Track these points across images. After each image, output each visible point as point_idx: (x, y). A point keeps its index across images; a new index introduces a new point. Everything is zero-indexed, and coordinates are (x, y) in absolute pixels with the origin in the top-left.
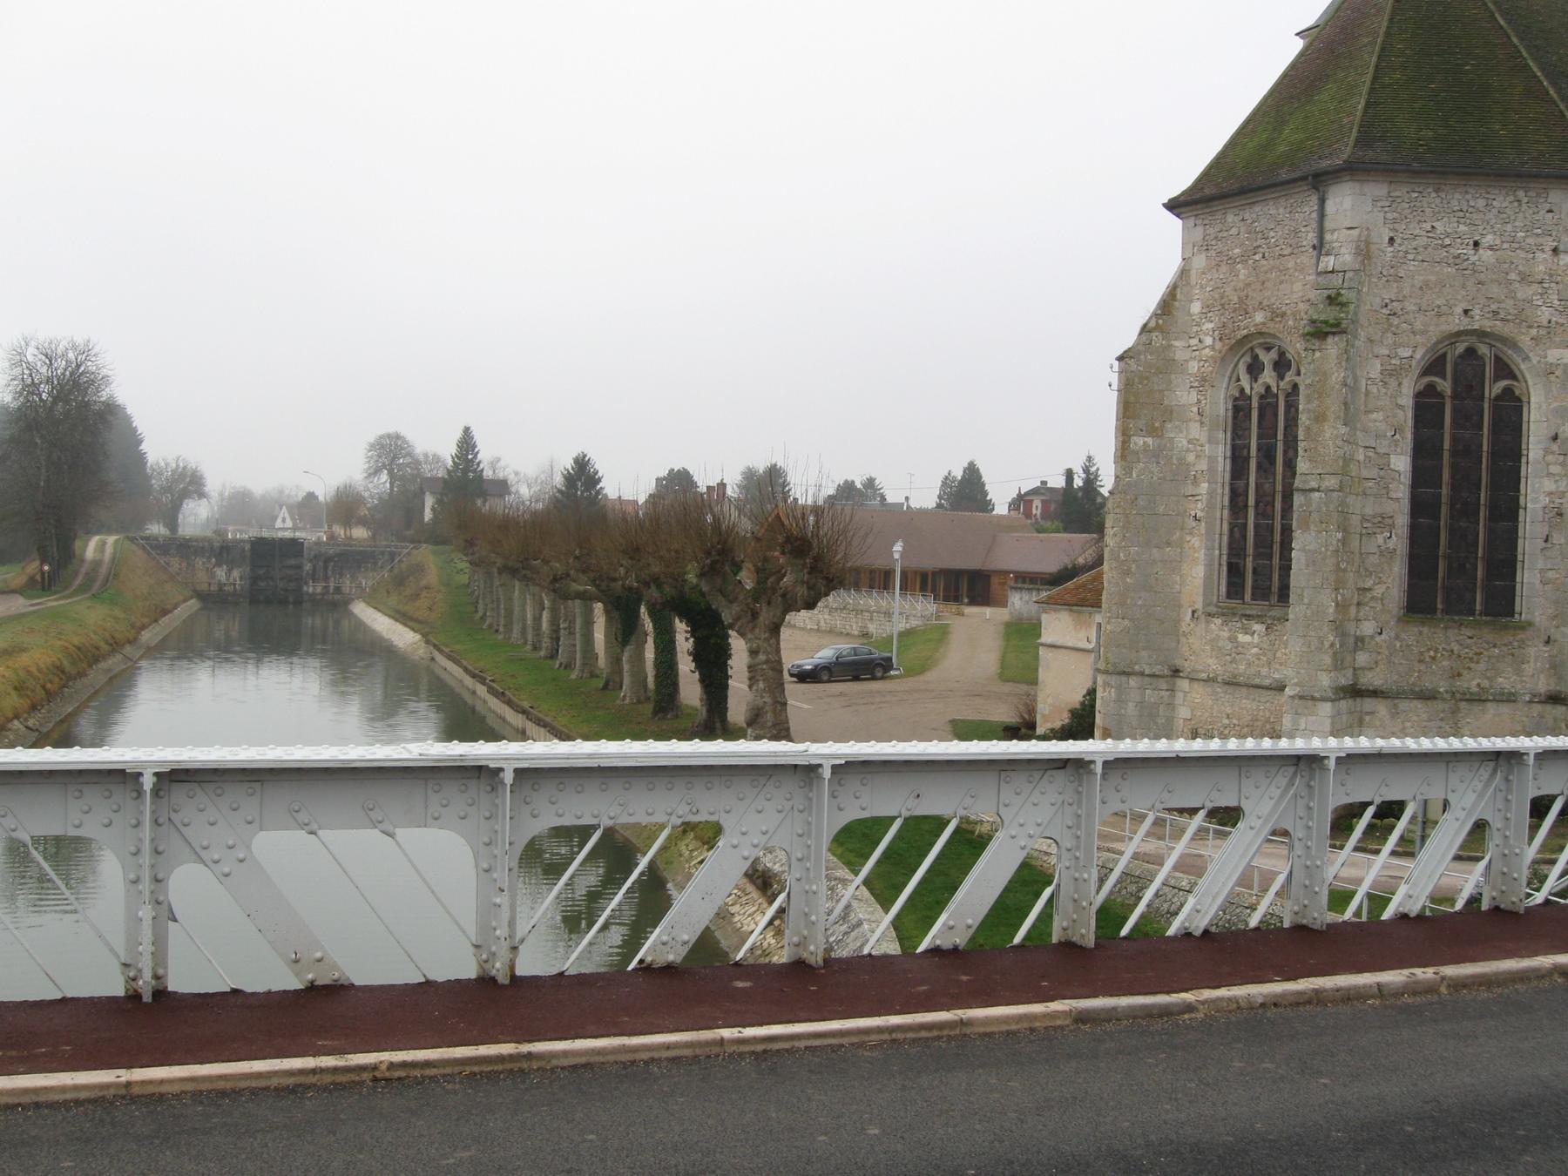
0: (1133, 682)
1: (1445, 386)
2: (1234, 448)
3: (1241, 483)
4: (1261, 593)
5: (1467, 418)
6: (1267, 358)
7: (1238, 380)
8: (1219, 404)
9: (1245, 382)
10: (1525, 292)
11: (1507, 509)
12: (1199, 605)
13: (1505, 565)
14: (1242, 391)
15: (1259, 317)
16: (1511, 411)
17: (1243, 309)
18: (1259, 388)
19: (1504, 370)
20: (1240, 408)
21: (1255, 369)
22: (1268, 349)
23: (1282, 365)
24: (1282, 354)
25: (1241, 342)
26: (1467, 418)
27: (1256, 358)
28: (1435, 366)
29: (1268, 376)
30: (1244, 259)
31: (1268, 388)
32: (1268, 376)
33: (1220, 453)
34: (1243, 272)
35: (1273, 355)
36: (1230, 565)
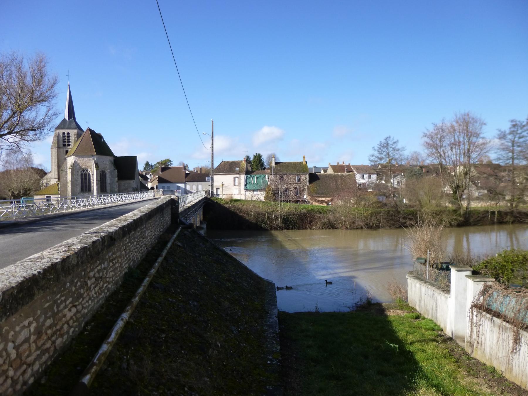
1: (102, 173)
4: (86, 190)
5: (103, 175)
8: (79, 173)
10: (107, 165)
11: (106, 183)
12: (79, 192)
13: (106, 187)
16: (105, 175)
18: (84, 172)
19: (105, 172)
20: (82, 174)
26: (103, 175)
28: (101, 172)
29: (85, 172)
33: (80, 178)
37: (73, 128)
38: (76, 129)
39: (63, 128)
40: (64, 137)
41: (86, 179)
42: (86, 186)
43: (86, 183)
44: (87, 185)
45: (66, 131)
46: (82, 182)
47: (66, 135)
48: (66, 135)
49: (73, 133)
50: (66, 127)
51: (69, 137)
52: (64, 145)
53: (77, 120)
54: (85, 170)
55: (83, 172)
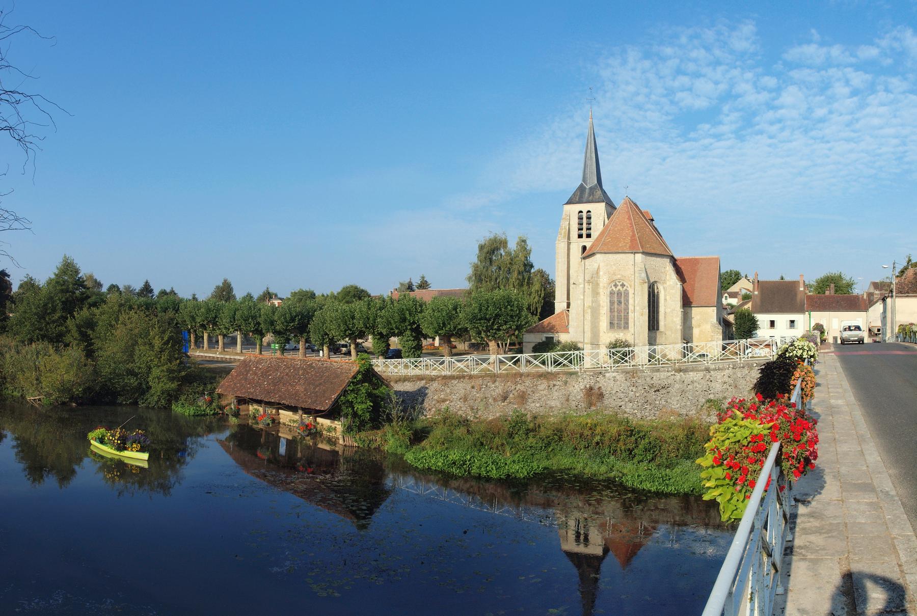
0: (594, 346)
2: (610, 300)
3: (613, 307)
6: (619, 284)
7: (611, 287)
9: (614, 288)
12: (605, 331)
14: (612, 289)
15: (619, 276)
17: (614, 274)
18: (617, 289)
20: (612, 293)
21: (616, 286)
22: (619, 282)
23: (623, 285)
24: (623, 283)
25: (614, 281)
27: (616, 283)
29: (619, 287)
30: (614, 265)
31: (619, 290)
32: (619, 287)
34: (614, 268)
35: (621, 283)
36: (610, 323)
37: (597, 200)
38: (603, 202)
39: (580, 202)
40: (581, 218)
41: (620, 302)
42: (619, 319)
43: (619, 311)
44: (621, 316)
45: (585, 207)
46: (612, 310)
47: (584, 215)
48: (584, 215)
49: (598, 210)
50: (584, 200)
51: (589, 218)
52: (580, 236)
53: (604, 187)
54: (619, 284)
55: (614, 289)
